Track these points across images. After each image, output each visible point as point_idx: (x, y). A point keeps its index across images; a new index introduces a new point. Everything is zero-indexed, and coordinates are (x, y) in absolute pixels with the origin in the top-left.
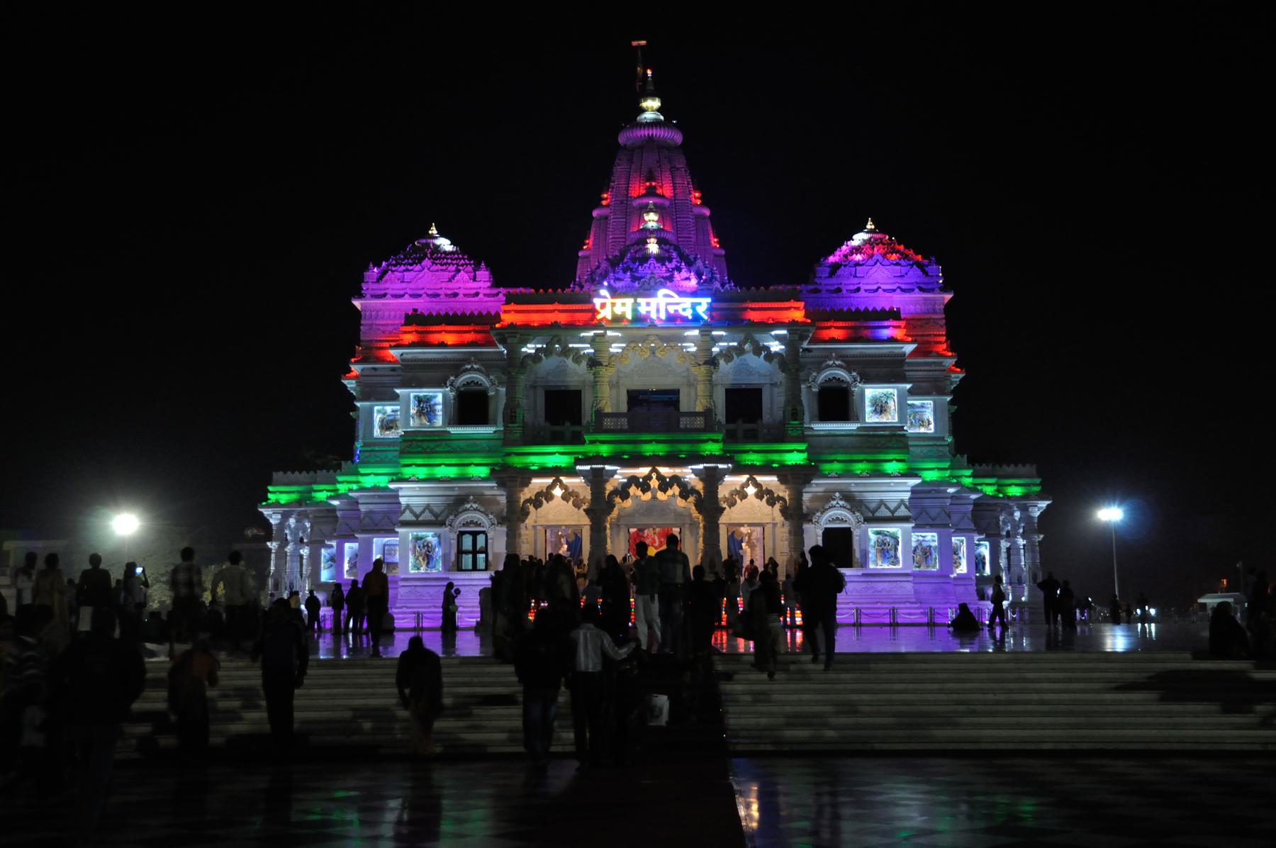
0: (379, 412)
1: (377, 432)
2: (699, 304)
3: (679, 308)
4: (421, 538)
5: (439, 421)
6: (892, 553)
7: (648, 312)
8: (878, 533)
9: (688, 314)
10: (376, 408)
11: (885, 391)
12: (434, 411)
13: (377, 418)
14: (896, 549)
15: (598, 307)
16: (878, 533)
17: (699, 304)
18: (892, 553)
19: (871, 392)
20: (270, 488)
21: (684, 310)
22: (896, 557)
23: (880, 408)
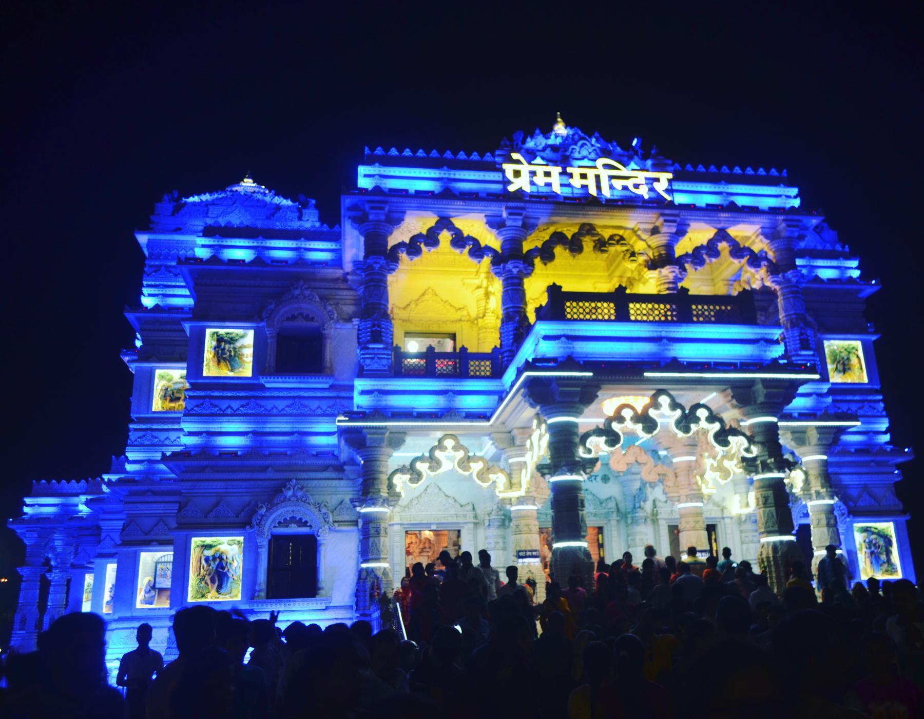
0: (162, 377)
1: (157, 405)
2: (657, 180)
3: (629, 183)
4: (209, 547)
5: (246, 371)
6: (883, 557)
7: (585, 187)
8: (866, 530)
9: (643, 191)
10: (158, 372)
11: (846, 343)
12: (240, 356)
13: (159, 386)
14: (888, 553)
15: (509, 175)
16: (866, 530)
17: (657, 180)
18: (883, 557)
19: (833, 345)
20: (28, 501)
21: (637, 186)
22: (889, 561)
23: (844, 366)
